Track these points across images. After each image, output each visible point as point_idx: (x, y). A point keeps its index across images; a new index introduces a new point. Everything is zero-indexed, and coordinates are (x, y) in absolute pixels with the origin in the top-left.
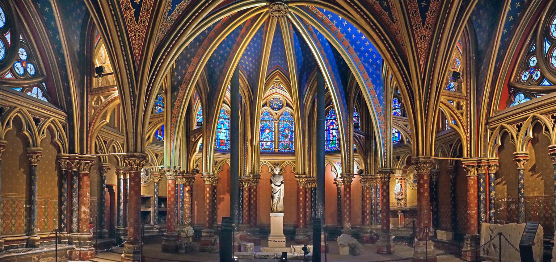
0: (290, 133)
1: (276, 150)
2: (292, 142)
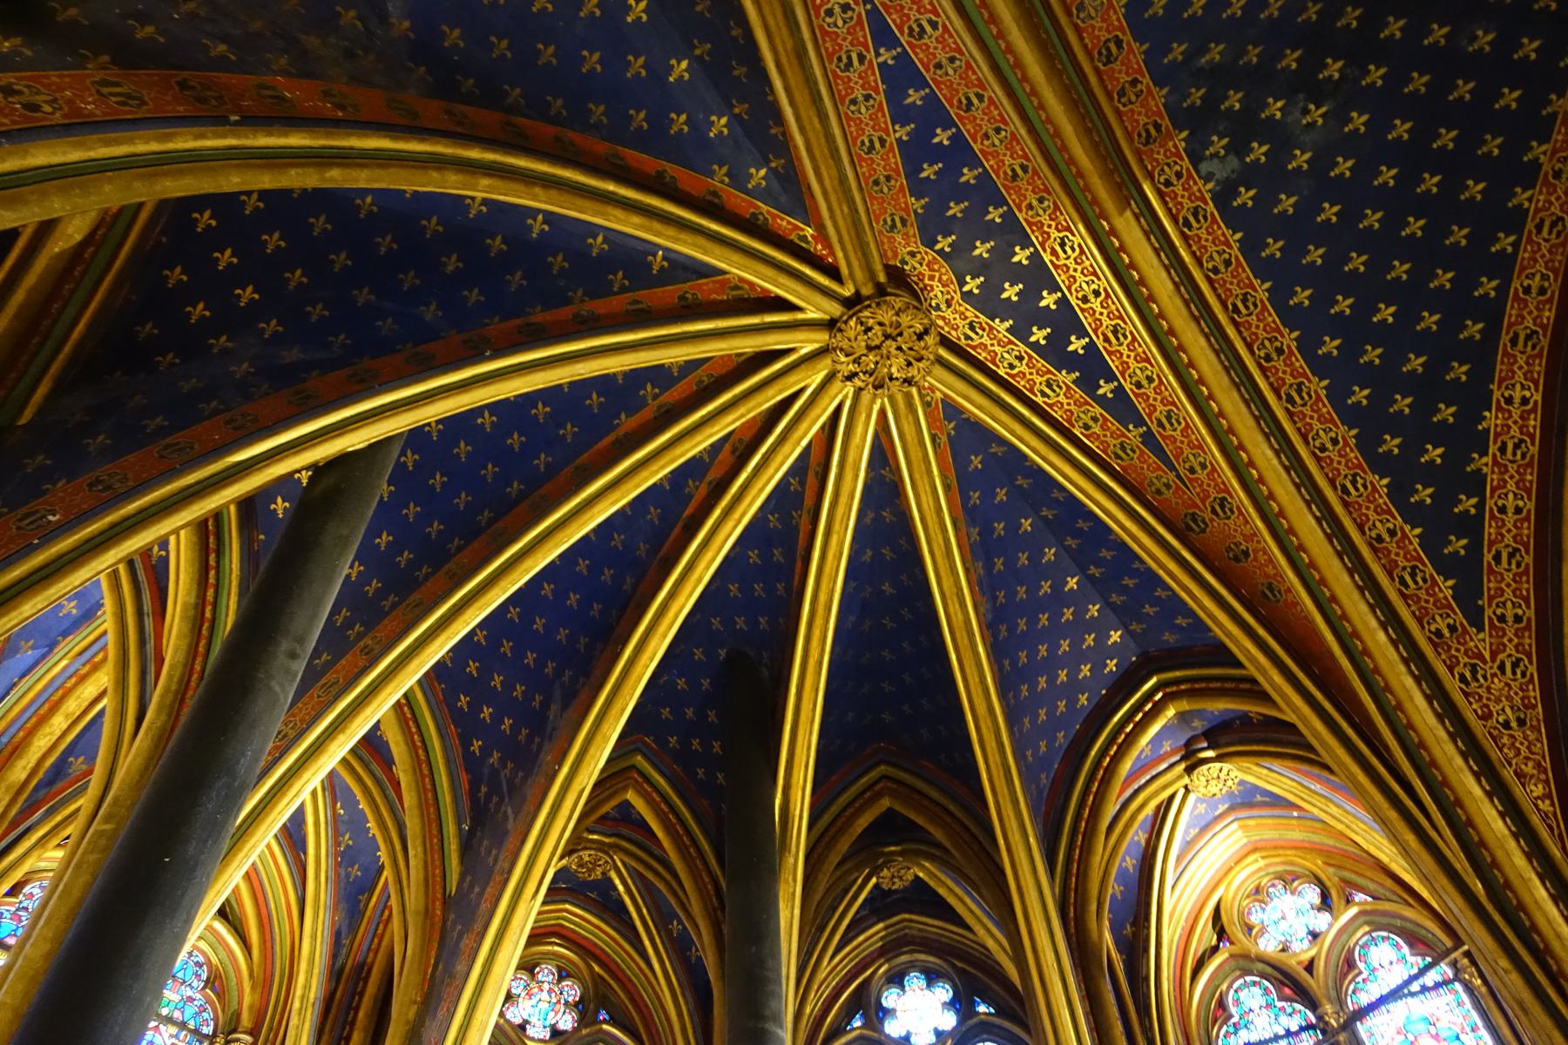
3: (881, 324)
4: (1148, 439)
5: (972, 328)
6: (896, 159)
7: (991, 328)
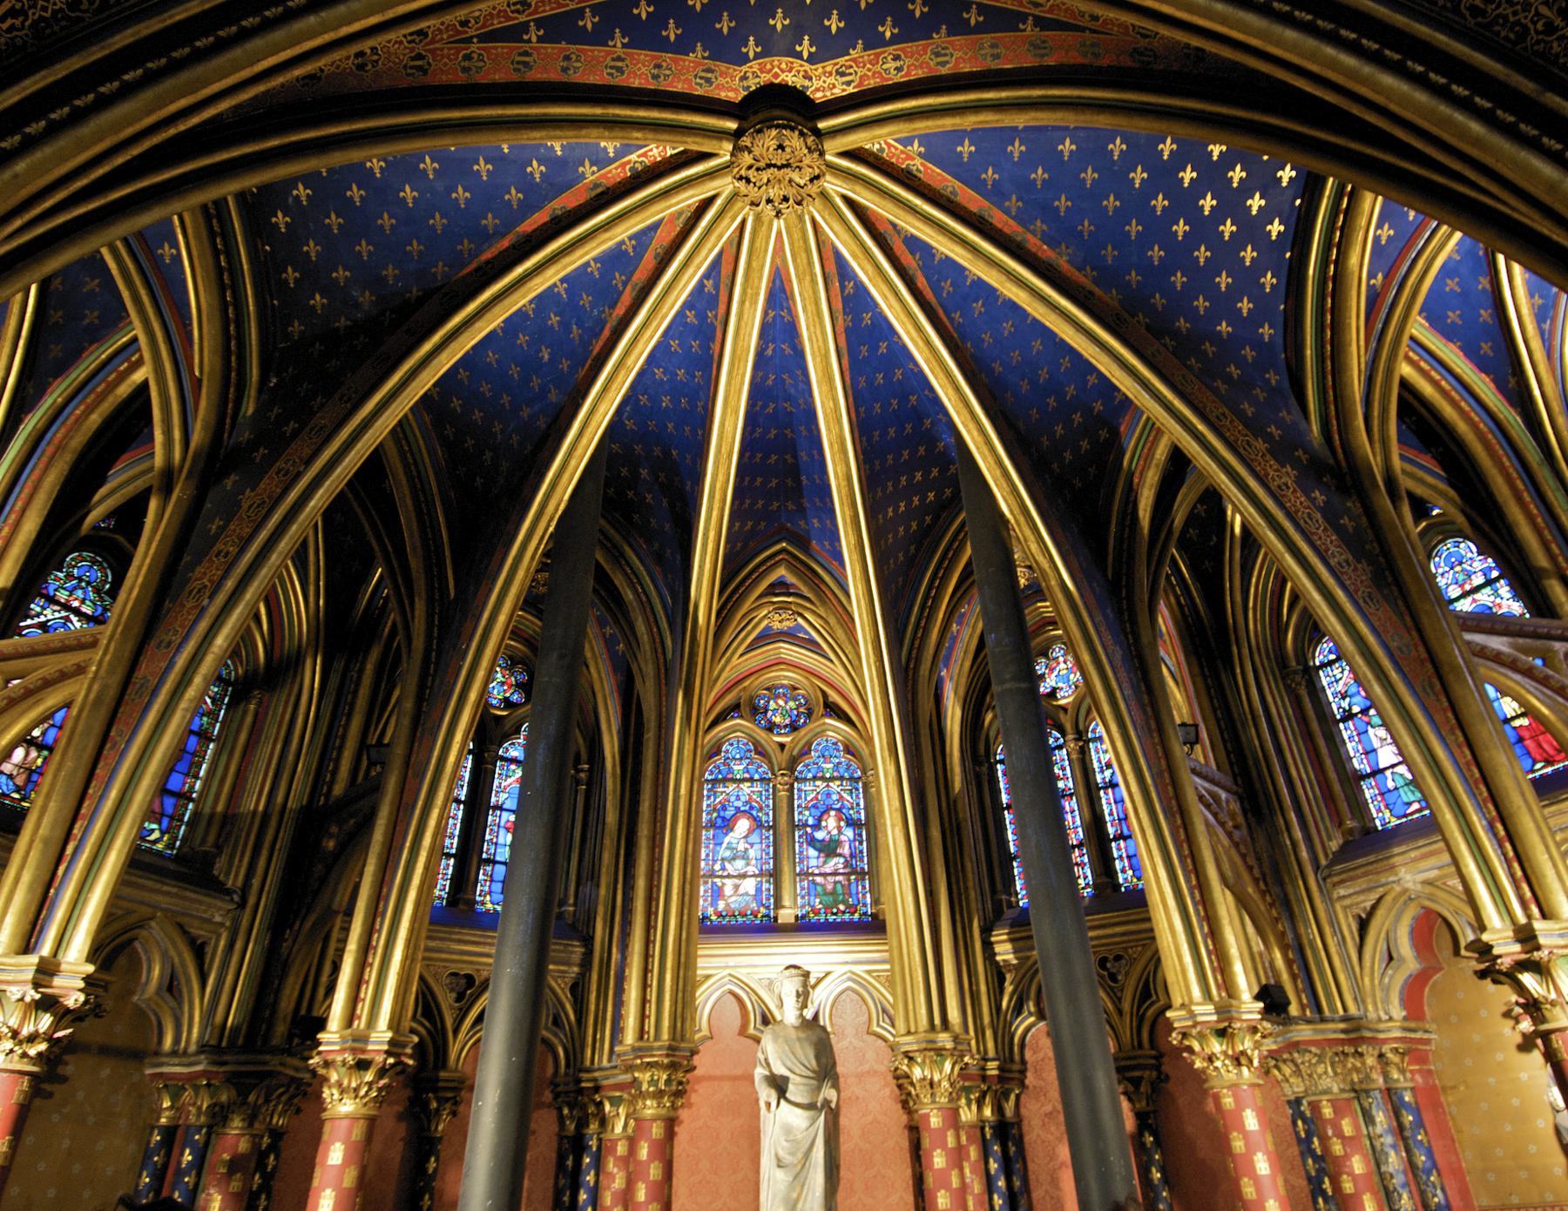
0: (849, 833)
1: (787, 915)
2: (861, 874)
3: (750, 167)
4: (1041, 23)
5: (843, 74)
6: (643, 55)
7: (854, 60)
